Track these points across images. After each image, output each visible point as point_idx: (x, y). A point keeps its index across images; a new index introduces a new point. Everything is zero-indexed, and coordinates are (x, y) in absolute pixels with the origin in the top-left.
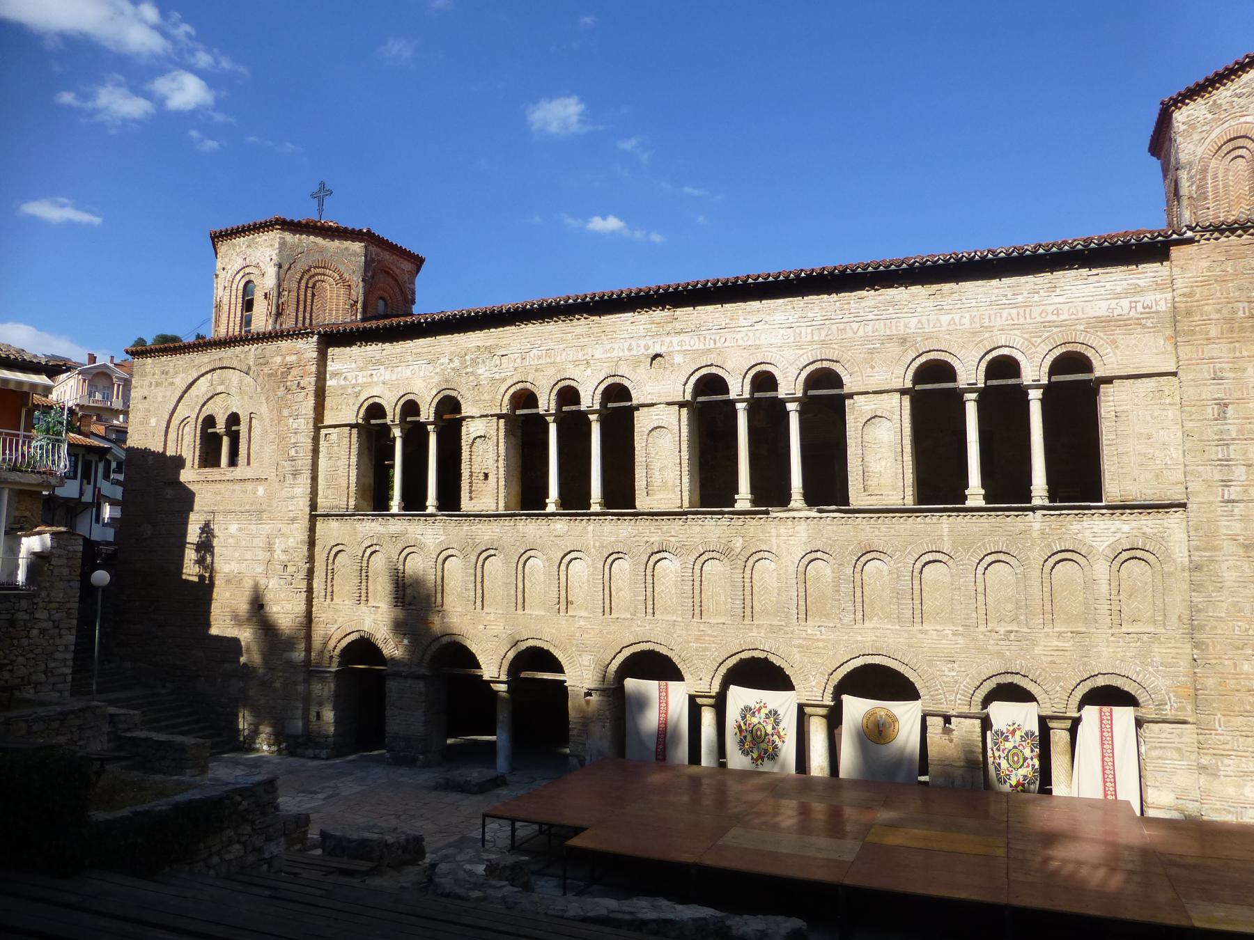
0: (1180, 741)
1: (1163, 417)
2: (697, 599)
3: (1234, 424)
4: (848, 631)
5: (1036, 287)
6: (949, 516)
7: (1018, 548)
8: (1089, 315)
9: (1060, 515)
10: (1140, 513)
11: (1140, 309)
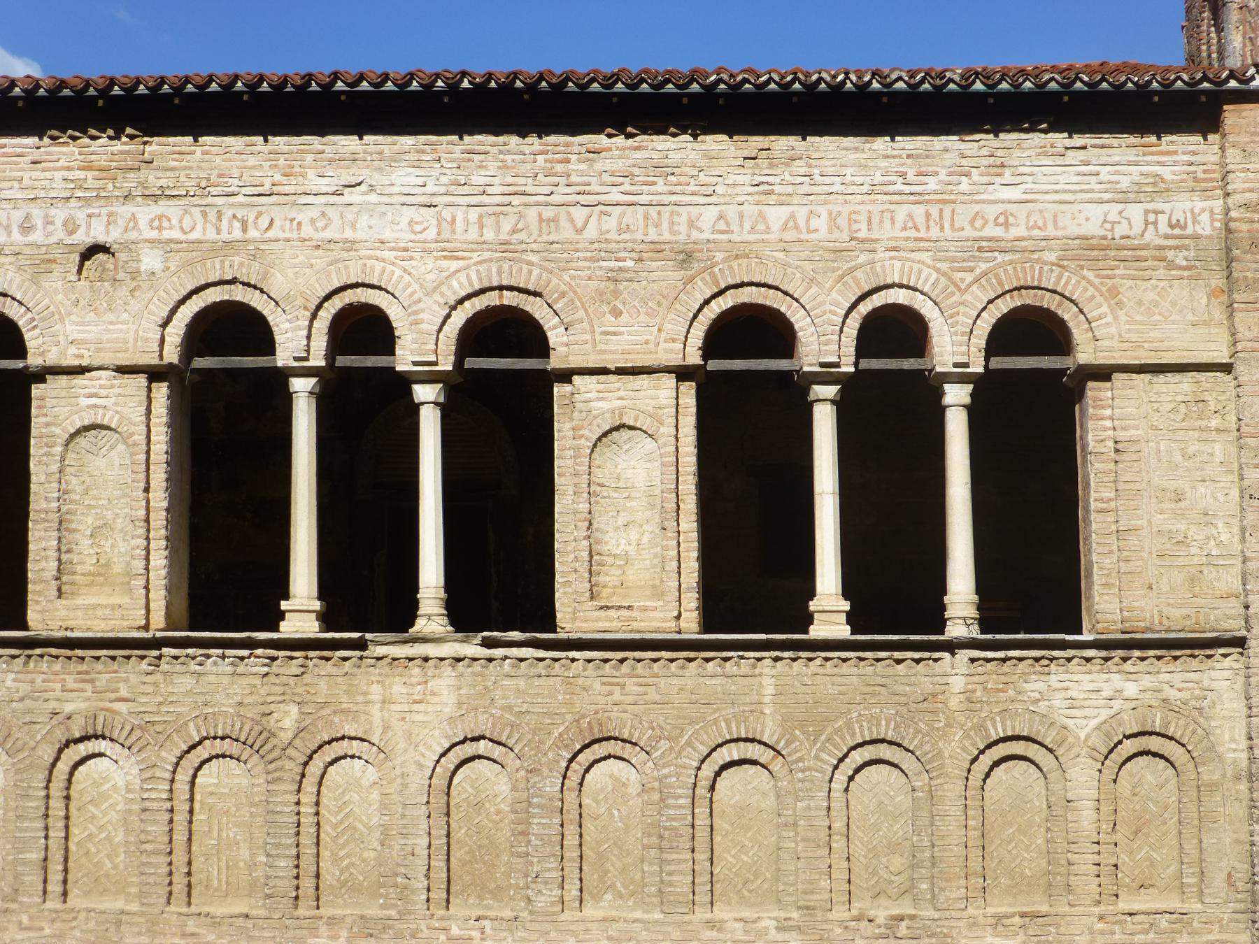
1: (1205, 458)
2: (180, 857)
4: (547, 926)
5: (964, 162)
6: (776, 659)
7: (918, 731)
8: (1068, 232)
9: (1004, 660)
10: (1159, 658)
11: (1163, 228)
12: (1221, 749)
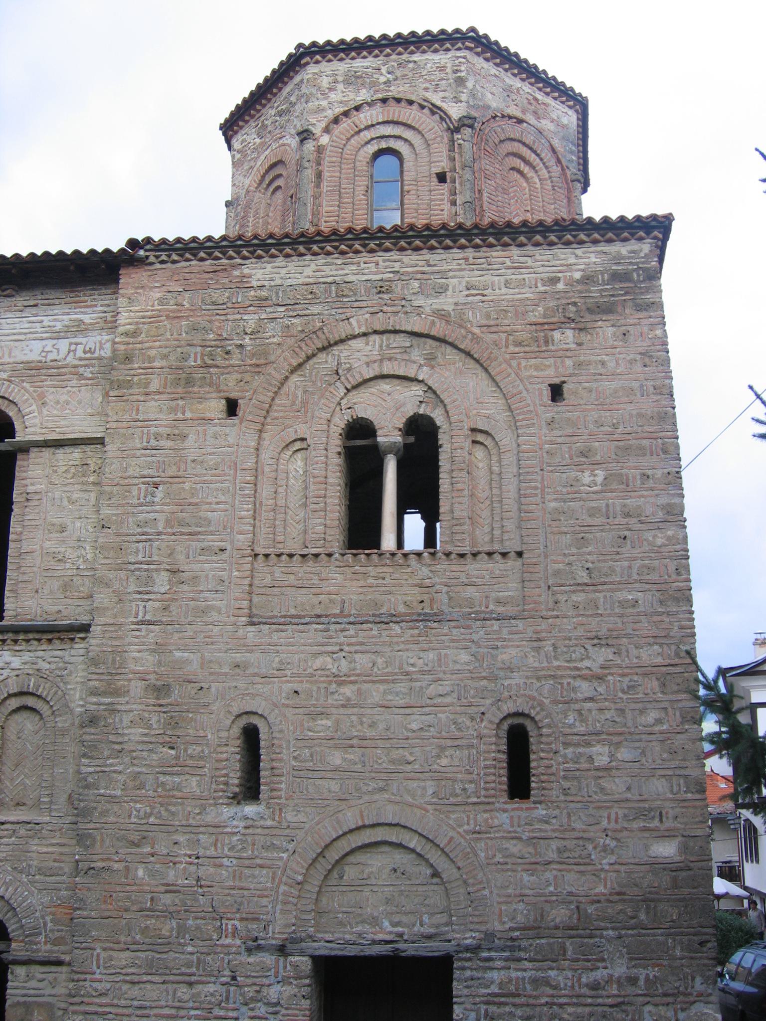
0: (53, 992)
1: (83, 502)
8: (18, 359)
11: (80, 353)
12: (72, 705)
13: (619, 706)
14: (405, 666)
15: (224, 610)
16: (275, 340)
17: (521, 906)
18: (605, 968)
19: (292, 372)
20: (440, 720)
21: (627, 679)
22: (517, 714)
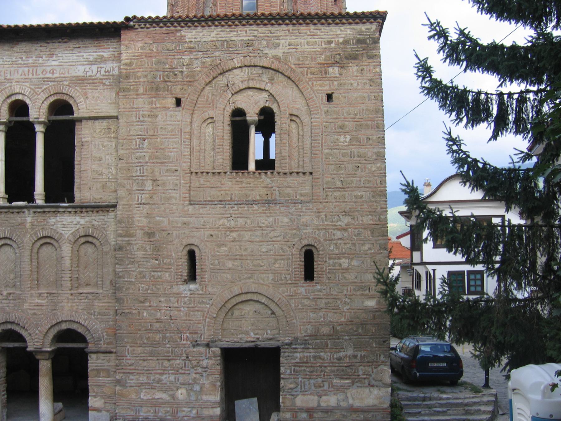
0: (109, 364)
1: (109, 146)
3: (147, 152)
5: (41, 53)
7: (17, 235)
11: (103, 72)
12: (110, 241)
13: (353, 242)
14: (260, 223)
15: (178, 198)
16: (198, 69)
17: (309, 327)
18: (344, 351)
19: (206, 85)
20: (275, 248)
21: (357, 230)
22: (309, 245)
